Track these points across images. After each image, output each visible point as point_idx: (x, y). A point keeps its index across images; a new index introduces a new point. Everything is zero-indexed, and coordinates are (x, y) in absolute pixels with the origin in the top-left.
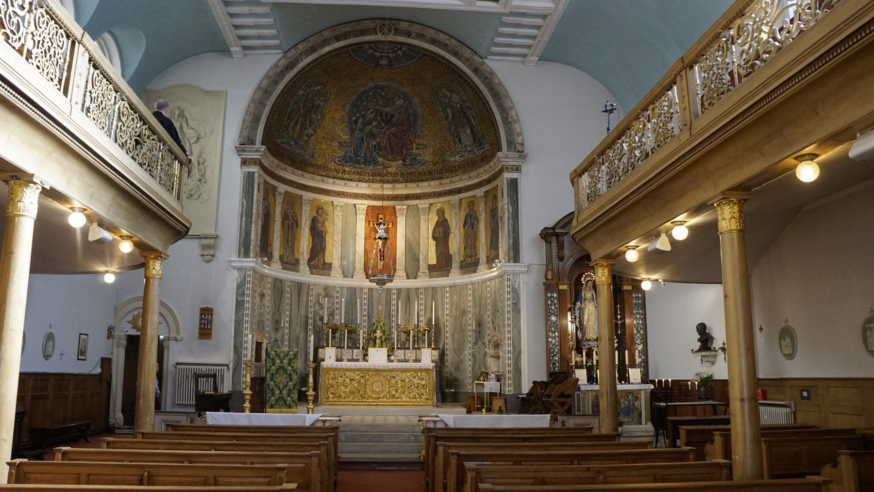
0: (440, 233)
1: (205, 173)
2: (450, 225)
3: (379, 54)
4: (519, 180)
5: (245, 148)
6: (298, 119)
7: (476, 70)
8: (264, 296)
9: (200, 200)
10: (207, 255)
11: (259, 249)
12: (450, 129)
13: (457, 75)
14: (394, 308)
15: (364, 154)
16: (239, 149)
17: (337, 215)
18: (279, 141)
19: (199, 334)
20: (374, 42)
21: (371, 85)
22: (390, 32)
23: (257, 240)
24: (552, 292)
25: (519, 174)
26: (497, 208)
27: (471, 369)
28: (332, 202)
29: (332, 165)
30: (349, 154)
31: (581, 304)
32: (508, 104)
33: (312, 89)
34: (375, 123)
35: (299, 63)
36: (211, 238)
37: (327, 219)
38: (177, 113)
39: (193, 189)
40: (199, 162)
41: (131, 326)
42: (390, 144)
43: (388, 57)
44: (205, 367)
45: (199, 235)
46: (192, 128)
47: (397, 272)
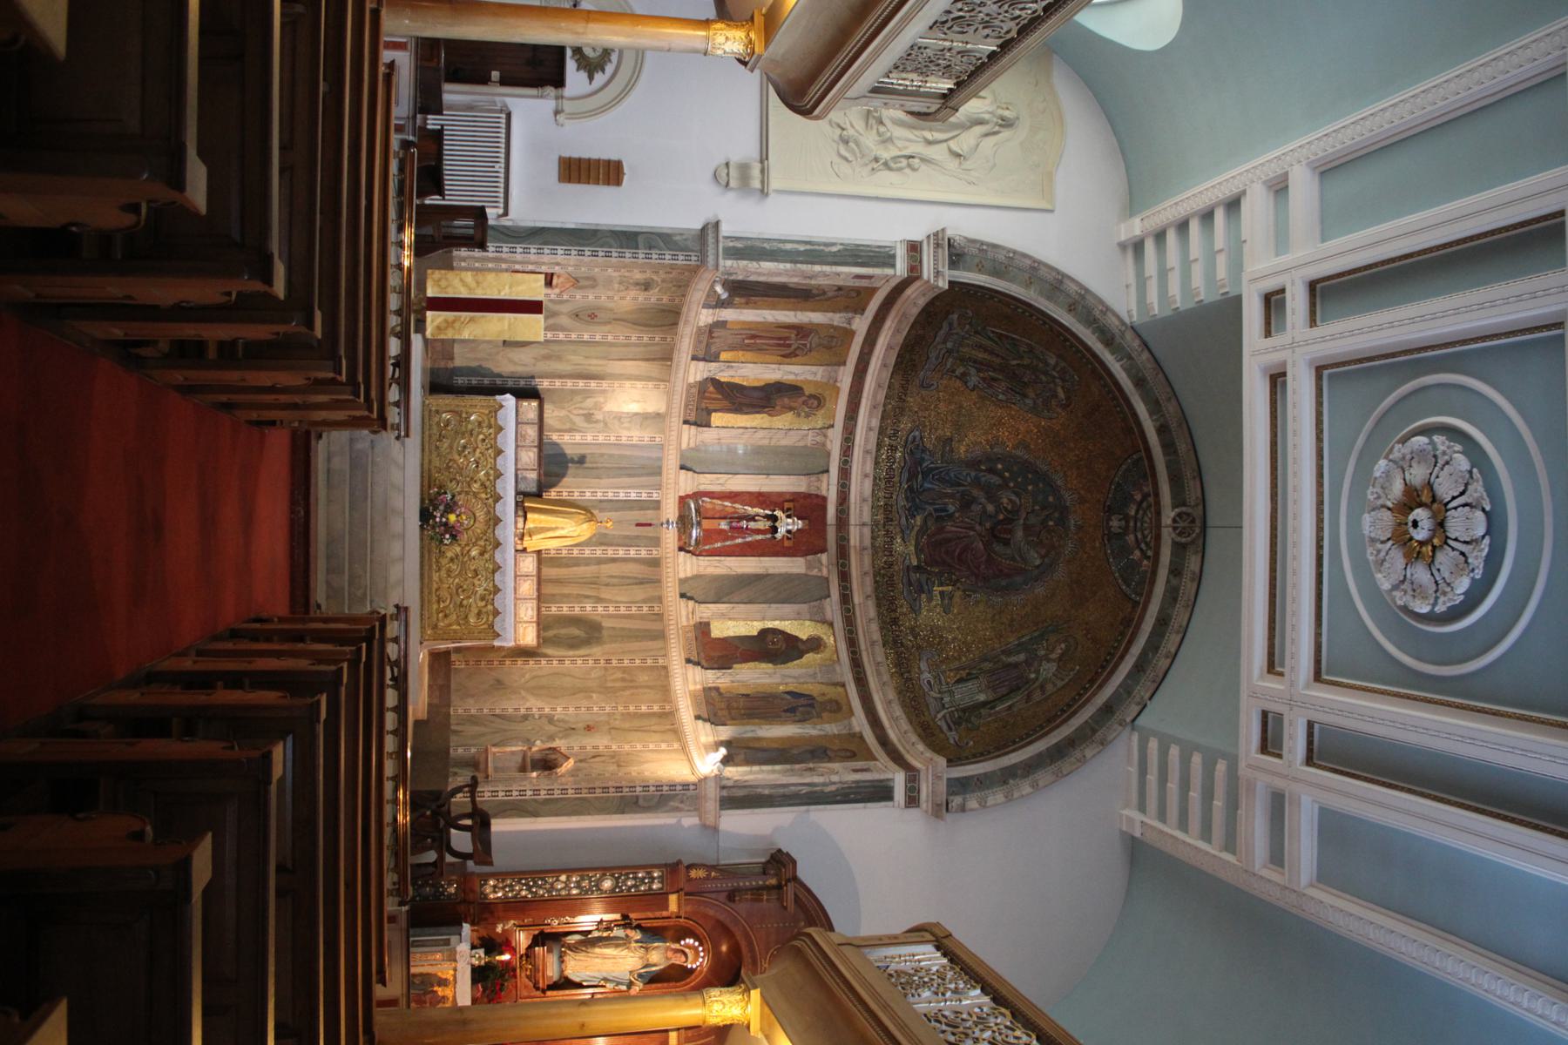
0: (773, 643)
1: (890, 169)
2: (790, 664)
3: (1133, 513)
4: (890, 804)
5: (943, 248)
6: (998, 356)
7: (1108, 710)
8: (646, 290)
9: (837, 160)
10: (728, 174)
11: (740, 278)
12: (985, 660)
13: (1097, 673)
14: (621, 553)
15: (929, 489)
16: (940, 235)
17: (807, 435)
18: (955, 316)
19: (570, 158)
20: (1158, 503)
21: (1068, 498)
22: (1180, 534)
23: (760, 274)
25: (902, 803)
26: (830, 760)
27: (498, 712)
28: (832, 426)
29: (905, 424)
30: (926, 457)
31: (637, 941)
32: (1043, 776)
33: (1058, 381)
34: (990, 508)
35: (1113, 354)
36: (762, 182)
37: (799, 415)
38: (1007, 113)
39: (857, 145)
40: (913, 157)
42: (950, 540)
43: (1126, 530)
44: (503, 170)
45: (767, 159)
46: (978, 145)
47: (694, 557)
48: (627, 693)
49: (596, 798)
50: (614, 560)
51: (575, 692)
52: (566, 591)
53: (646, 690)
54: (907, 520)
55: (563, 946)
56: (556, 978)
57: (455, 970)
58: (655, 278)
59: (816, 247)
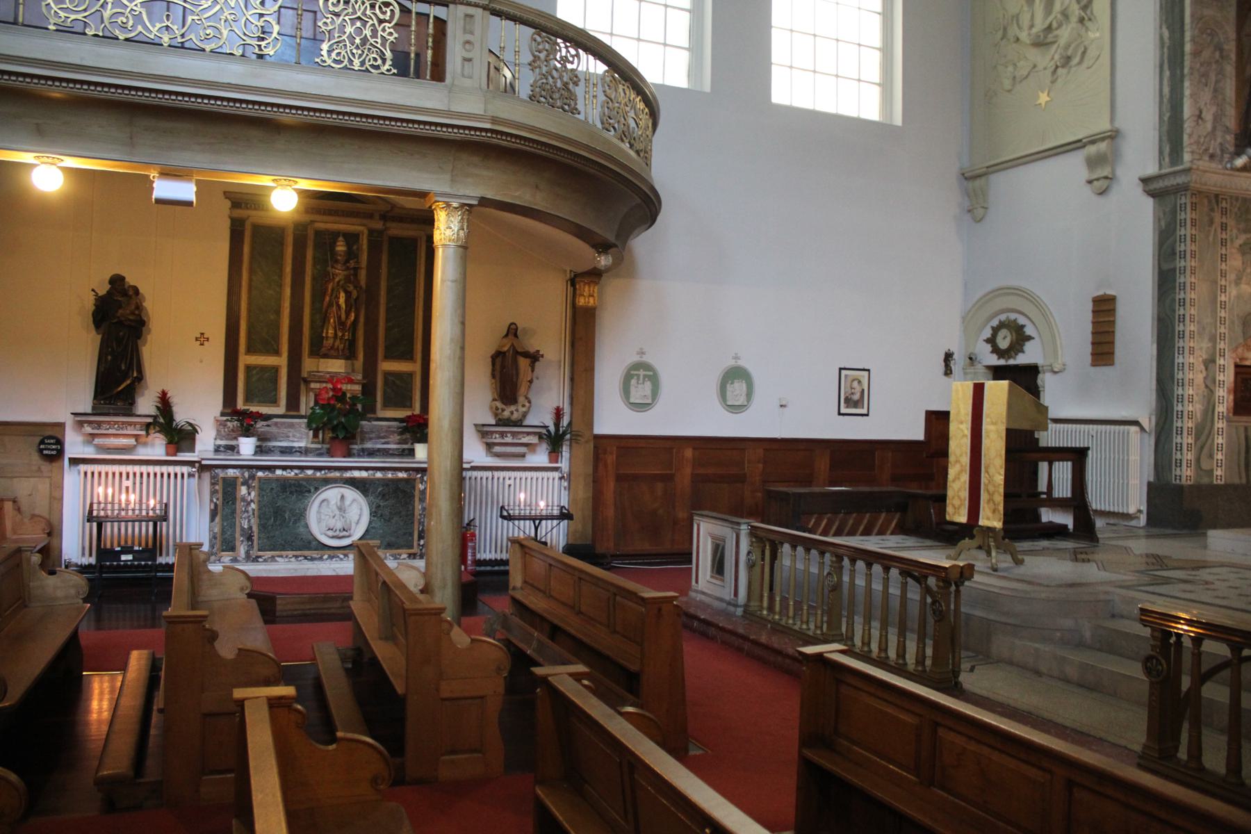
9: (1085, 64)
10: (1097, 179)
11: (1230, 138)
23: (1217, 118)
36: (1103, 139)
41: (989, 347)
58: (1239, 242)
59: (1166, 56)
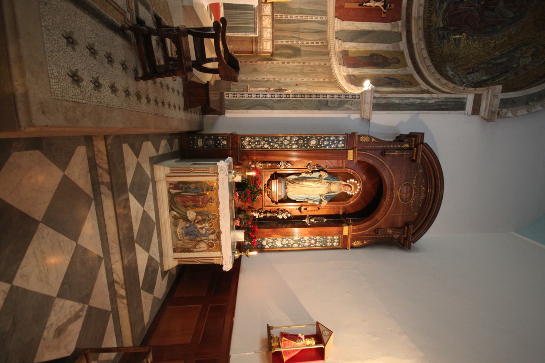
4: (463, 112)
14: (309, 18)
24: (344, 142)
27: (254, 79)
31: (325, 179)
47: (342, 21)
48: (314, 75)
49: (305, 100)
50: (306, 21)
51: (289, 74)
52: (285, 34)
53: (322, 74)
54: (440, 5)
55: (286, 180)
56: (283, 197)
57: (218, 180)
